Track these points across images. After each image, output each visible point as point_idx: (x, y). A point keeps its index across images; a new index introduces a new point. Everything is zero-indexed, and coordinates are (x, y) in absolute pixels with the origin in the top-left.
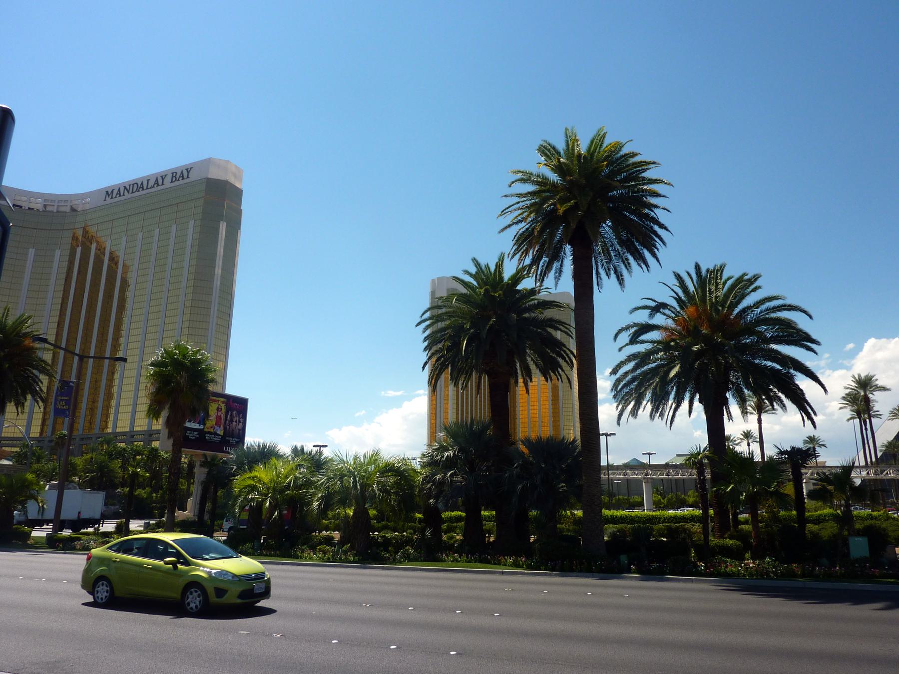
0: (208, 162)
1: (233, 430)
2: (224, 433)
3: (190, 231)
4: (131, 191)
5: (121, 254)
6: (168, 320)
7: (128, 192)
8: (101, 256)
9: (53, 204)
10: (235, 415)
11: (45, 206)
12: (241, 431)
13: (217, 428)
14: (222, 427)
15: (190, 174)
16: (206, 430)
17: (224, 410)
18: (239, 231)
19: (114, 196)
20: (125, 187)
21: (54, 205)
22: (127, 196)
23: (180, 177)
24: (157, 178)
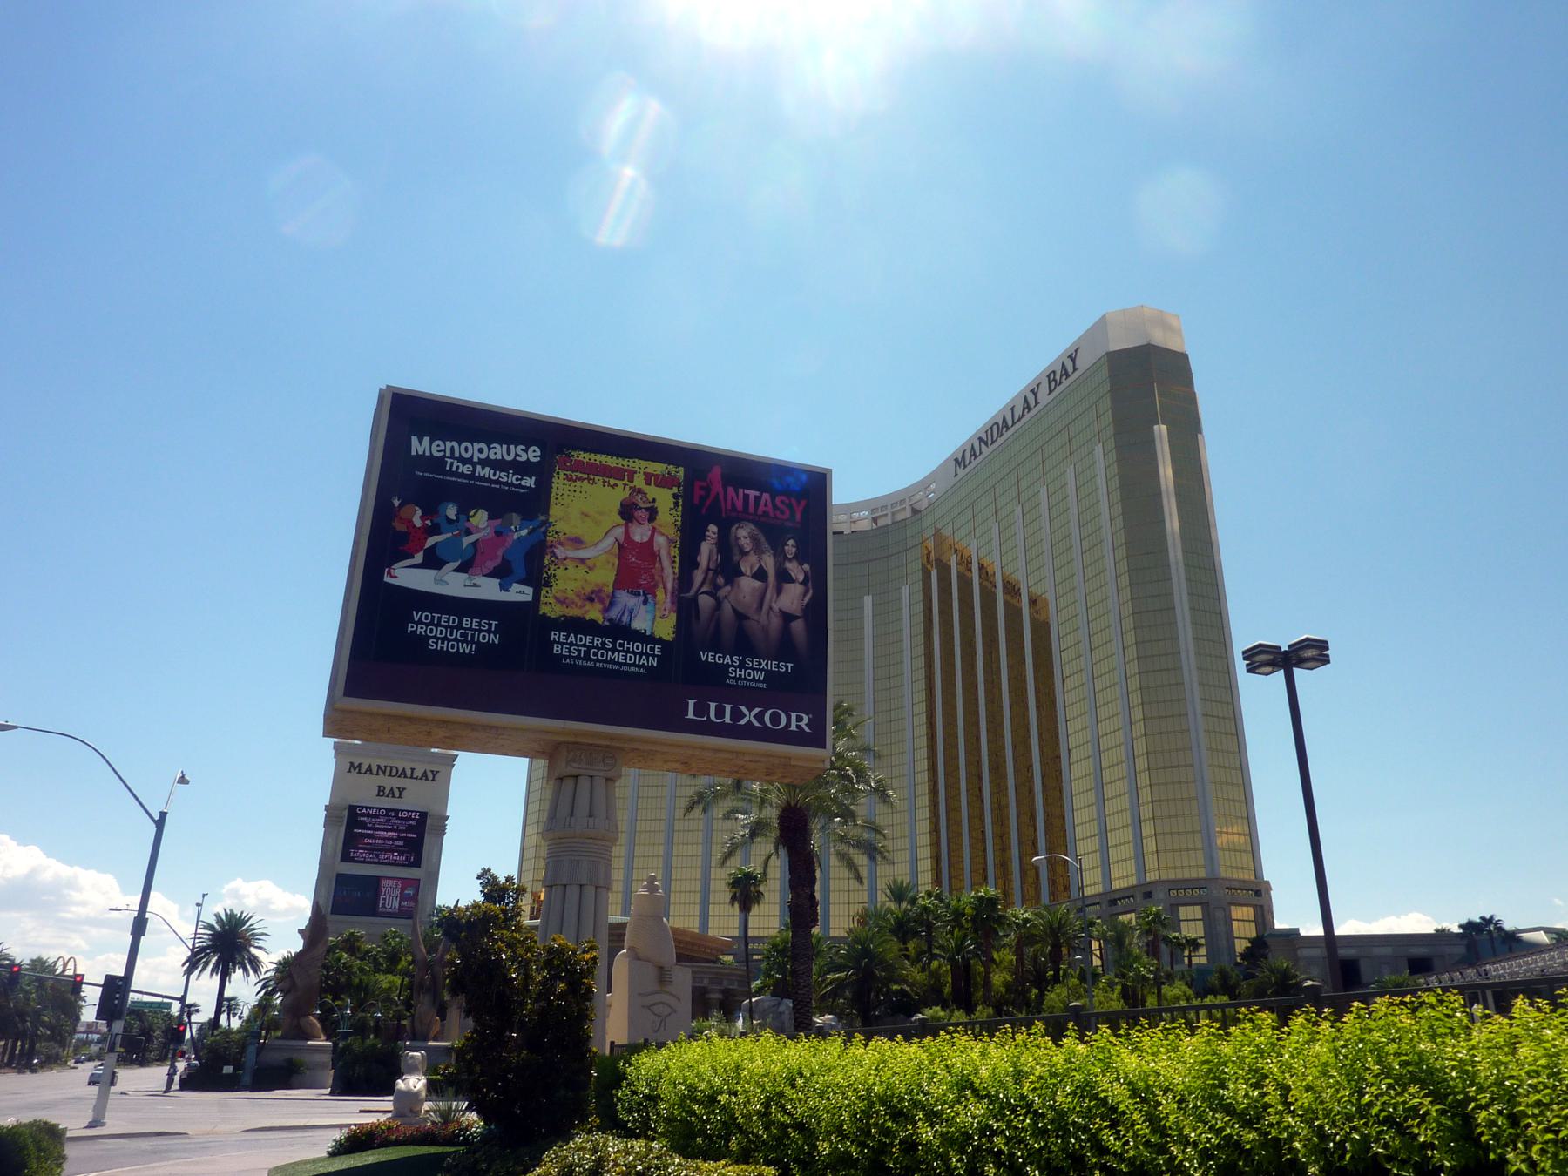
0: (1102, 324)
1: (740, 617)
2: (679, 628)
3: (1100, 465)
4: (990, 442)
5: (1020, 577)
6: (1097, 656)
7: (986, 444)
8: (993, 589)
9: (885, 513)
10: (746, 544)
11: (875, 520)
12: (798, 626)
13: (625, 598)
14: (663, 597)
15: (1077, 363)
16: (549, 608)
17: (669, 514)
18: (1199, 435)
19: (967, 462)
20: (980, 439)
21: (886, 515)
23: (1061, 376)
24: (1025, 398)
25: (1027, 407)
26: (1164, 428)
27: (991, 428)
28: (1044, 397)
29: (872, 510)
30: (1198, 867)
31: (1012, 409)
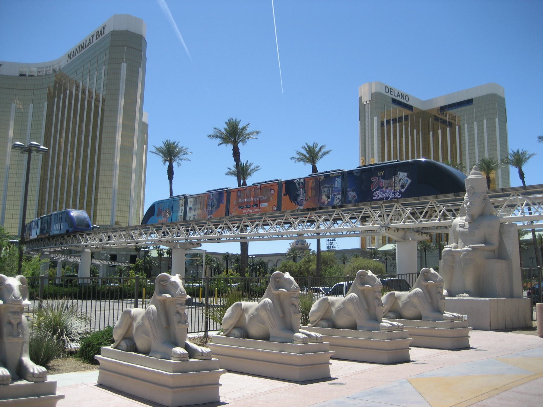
20: (76, 49)
22: (77, 55)
25: (90, 42)
26: (126, 65)
27: (80, 46)
28: (95, 41)
29: (38, 68)
30: (108, 221)
31: (86, 41)
